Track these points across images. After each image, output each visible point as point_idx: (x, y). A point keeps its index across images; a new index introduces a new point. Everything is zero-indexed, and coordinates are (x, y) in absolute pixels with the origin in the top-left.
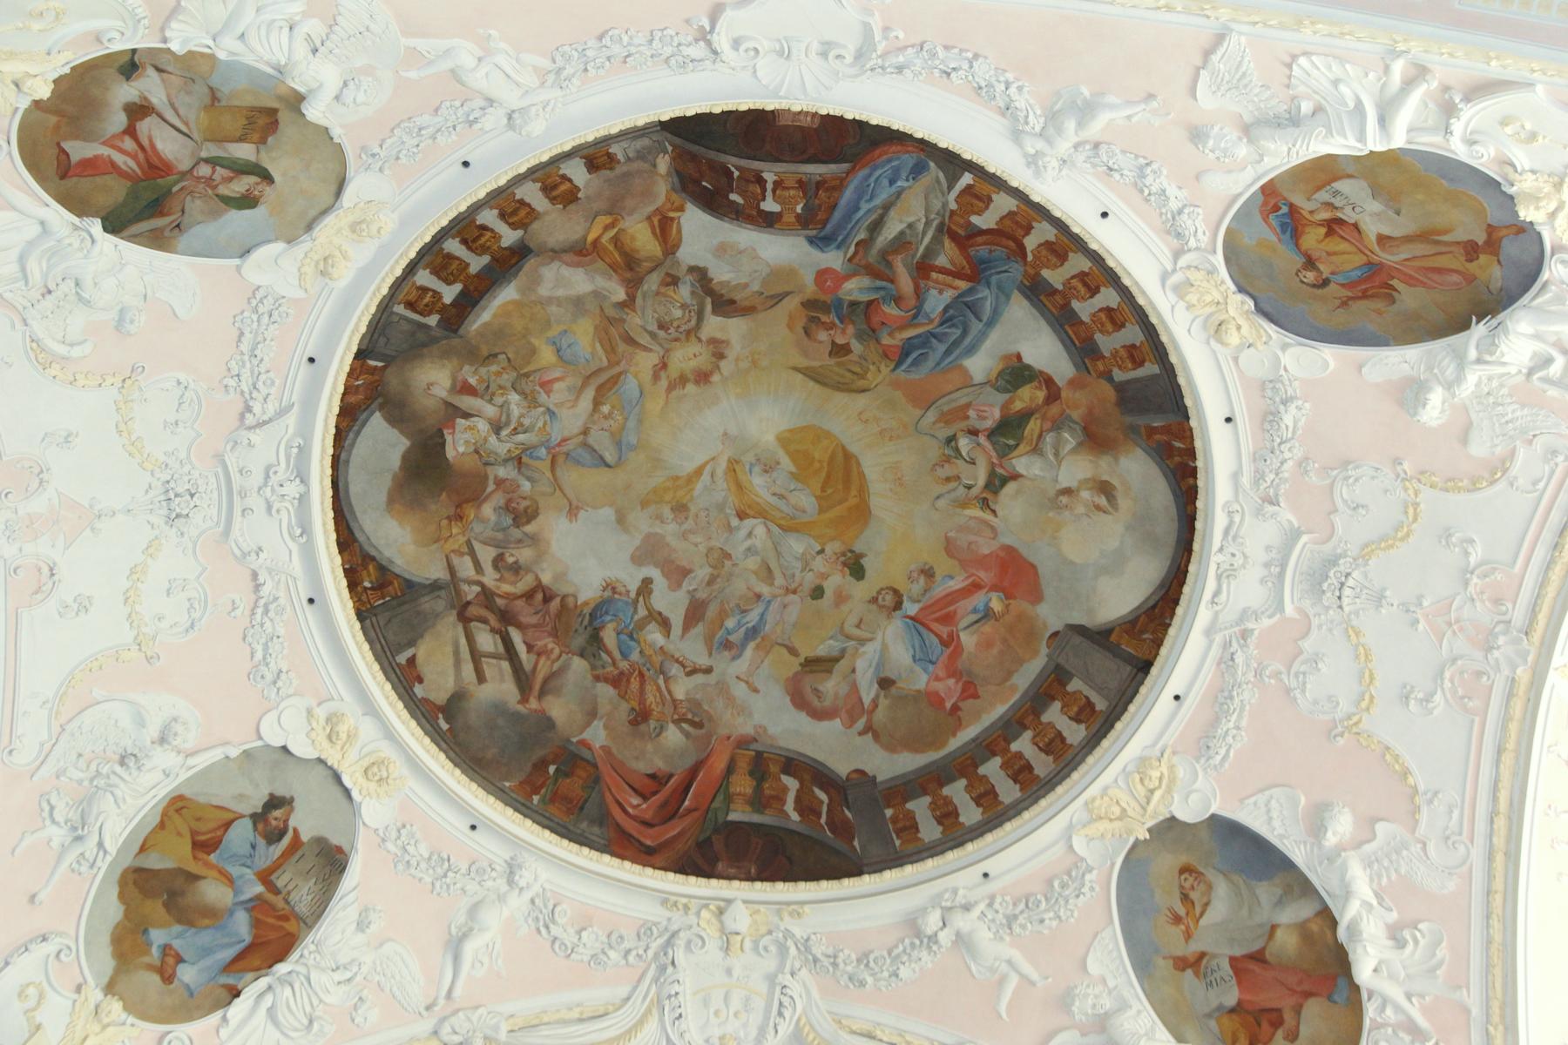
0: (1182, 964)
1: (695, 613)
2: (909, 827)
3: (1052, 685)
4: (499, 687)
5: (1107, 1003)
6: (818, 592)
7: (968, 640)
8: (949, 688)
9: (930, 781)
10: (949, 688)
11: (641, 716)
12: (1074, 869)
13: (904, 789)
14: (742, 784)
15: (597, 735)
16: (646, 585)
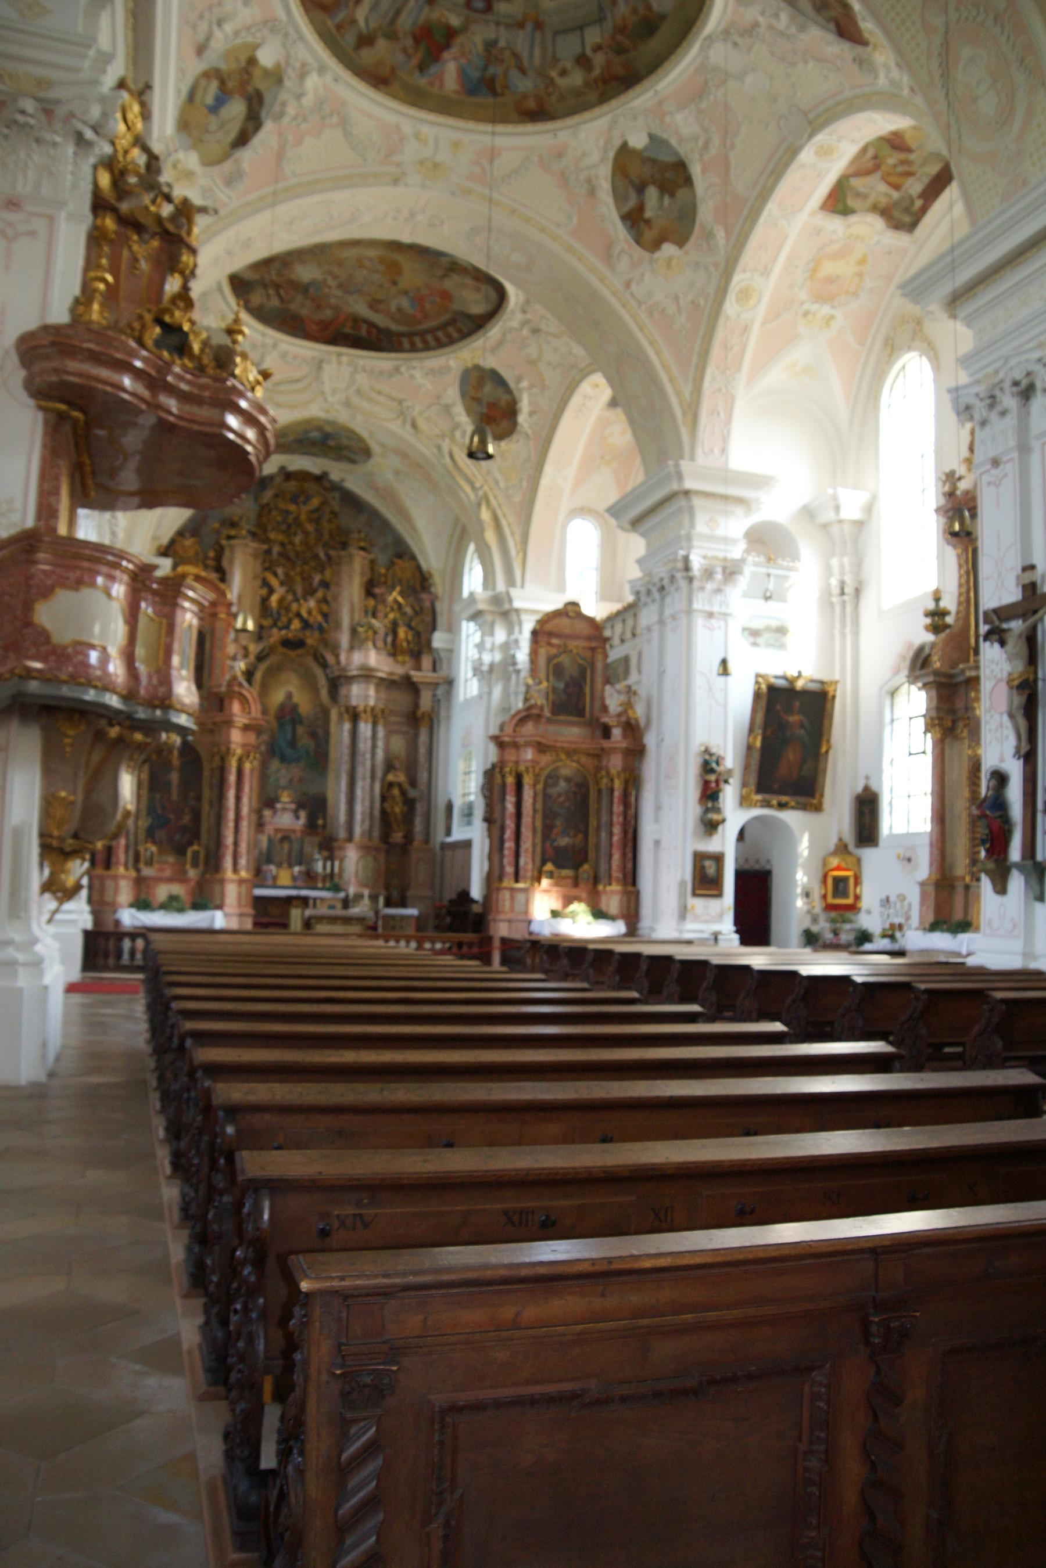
0: (474, 399)
1: (340, 286)
2: (400, 344)
3: (452, 322)
4: (275, 302)
5: (450, 401)
6: (381, 286)
7: (428, 306)
8: (419, 315)
9: (410, 335)
10: (419, 315)
11: (319, 307)
12: (447, 369)
13: (401, 335)
14: (349, 324)
15: (304, 312)
16: (325, 280)
